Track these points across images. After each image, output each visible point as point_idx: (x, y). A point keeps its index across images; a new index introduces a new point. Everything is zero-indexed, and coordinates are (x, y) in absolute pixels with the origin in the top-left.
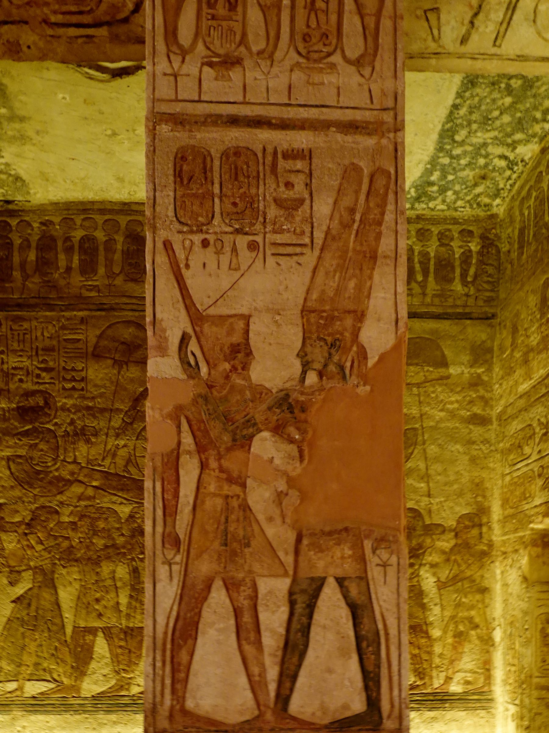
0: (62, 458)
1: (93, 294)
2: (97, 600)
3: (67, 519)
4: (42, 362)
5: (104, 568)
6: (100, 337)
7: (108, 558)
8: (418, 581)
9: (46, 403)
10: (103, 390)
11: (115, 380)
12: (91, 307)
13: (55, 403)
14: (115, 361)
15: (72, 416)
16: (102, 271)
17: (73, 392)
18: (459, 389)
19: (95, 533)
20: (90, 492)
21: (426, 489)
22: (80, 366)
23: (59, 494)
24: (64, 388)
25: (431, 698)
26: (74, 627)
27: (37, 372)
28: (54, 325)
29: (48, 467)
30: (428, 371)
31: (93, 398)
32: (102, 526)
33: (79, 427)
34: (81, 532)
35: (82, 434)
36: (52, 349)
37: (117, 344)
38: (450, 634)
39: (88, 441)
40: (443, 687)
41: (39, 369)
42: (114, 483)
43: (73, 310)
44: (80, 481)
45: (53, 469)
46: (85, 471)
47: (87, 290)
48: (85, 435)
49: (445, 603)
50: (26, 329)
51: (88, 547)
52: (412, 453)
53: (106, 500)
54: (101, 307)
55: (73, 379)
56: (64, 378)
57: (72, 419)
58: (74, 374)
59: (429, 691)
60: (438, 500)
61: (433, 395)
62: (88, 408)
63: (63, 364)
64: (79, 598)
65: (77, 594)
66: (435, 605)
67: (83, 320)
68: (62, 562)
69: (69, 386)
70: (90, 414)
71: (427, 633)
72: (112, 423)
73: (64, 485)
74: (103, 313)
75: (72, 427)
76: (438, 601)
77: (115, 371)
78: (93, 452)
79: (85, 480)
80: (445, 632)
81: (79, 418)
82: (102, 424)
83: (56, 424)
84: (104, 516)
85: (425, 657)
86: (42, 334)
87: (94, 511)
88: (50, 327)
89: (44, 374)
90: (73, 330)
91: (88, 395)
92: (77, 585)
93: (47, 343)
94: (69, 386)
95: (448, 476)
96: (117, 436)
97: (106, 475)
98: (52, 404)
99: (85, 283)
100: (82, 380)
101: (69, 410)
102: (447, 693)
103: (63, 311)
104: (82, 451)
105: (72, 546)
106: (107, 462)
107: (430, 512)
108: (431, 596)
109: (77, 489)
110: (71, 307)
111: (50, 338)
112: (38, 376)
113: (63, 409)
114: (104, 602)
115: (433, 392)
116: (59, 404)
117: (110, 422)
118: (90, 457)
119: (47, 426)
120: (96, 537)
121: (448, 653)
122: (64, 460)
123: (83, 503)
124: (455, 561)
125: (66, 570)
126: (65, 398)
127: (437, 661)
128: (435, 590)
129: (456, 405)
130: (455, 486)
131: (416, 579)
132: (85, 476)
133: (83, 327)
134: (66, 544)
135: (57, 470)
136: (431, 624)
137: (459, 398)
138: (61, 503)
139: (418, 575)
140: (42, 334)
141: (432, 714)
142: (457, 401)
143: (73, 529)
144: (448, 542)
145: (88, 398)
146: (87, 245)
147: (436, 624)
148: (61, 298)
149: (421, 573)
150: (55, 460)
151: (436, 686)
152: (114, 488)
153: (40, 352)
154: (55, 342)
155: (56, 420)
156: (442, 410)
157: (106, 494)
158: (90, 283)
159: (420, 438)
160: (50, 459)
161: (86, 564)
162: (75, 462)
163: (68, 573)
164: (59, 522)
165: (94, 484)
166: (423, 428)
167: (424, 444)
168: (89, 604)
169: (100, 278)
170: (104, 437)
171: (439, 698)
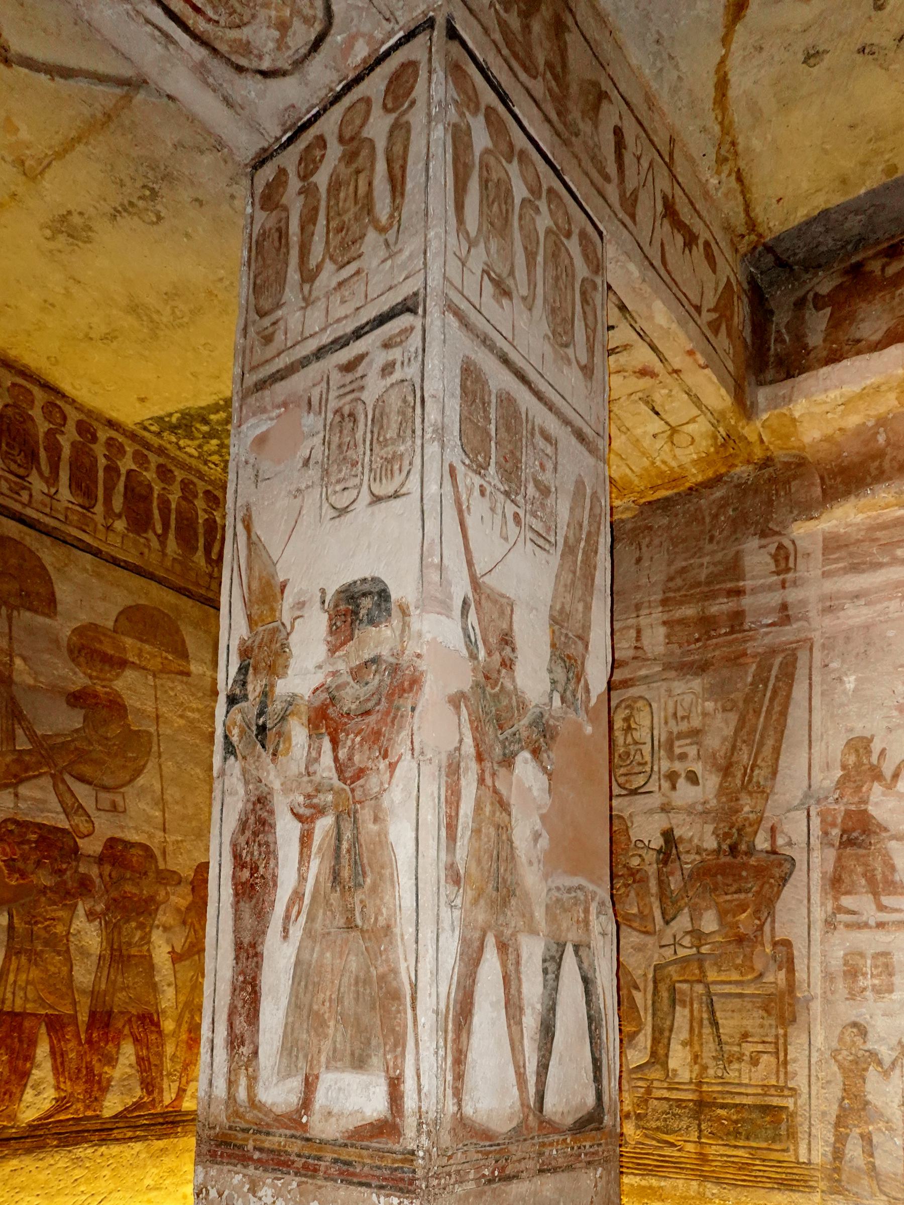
8: (148, 950)
18: (200, 694)
21: (160, 820)
25: (161, 1120)
30: (166, 658)
38: (185, 1027)
40: (175, 1103)
49: (180, 984)
52: (144, 766)
59: (159, 1110)
60: (173, 838)
61: (172, 694)
66: (169, 985)
71: (158, 1025)
76: (172, 979)
80: (179, 1025)
85: (154, 1060)
95: (185, 807)
102: (179, 1113)
107: (164, 853)
108: (164, 972)
115: (172, 689)
121: (182, 1055)
124: (192, 924)
127: (168, 1065)
128: (169, 964)
129: (197, 715)
130: (194, 824)
131: (146, 947)
136: (164, 1012)
137: (200, 706)
139: (149, 942)
141: (161, 1144)
142: (198, 710)
144: (184, 898)
147: (169, 1013)
149: (154, 938)
151: (166, 1102)
156: (181, 716)
159: (155, 748)
166: (159, 735)
167: (160, 756)
171: (171, 1119)
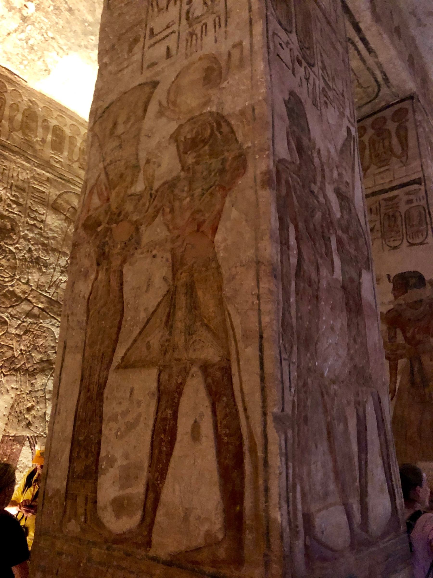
0: (18, 277)
1: (58, 165)
2: (29, 410)
3: (14, 331)
4: (14, 196)
5: (38, 380)
6: (59, 196)
7: (42, 371)
9: (13, 229)
10: (55, 235)
11: (65, 231)
12: (56, 174)
13: (19, 231)
14: (67, 218)
15: (30, 246)
16: (66, 154)
17: (34, 228)
19: (35, 348)
20: (36, 311)
22: (42, 211)
23: (10, 307)
24: (27, 223)
26: (4, 436)
27: (9, 202)
28: (27, 174)
29: (6, 282)
31: (48, 238)
32: (41, 343)
33: (35, 257)
34: (24, 345)
35: (37, 262)
36: (23, 190)
37: (69, 207)
39: (40, 270)
41: (11, 200)
42: (55, 310)
43: (44, 170)
44: (29, 301)
45: (9, 284)
46: (35, 294)
47: (55, 161)
48: (39, 264)
50: (5, 166)
51: (27, 359)
53: (47, 321)
54: (61, 176)
55: (35, 219)
56: (29, 216)
57: (30, 249)
58: (37, 215)
62: (43, 244)
63: (30, 205)
64: (12, 406)
65: (11, 402)
67: (48, 179)
68: (4, 370)
69: (32, 222)
70: (44, 250)
72: (60, 262)
73: (16, 301)
74: (63, 182)
75: (29, 255)
77: (66, 225)
78: (43, 279)
79: (34, 301)
81: (36, 250)
82: (52, 260)
83: (17, 248)
84: (44, 334)
86: (18, 175)
87: (36, 329)
88: (24, 174)
89: (14, 206)
90: (40, 183)
91: (45, 234)
92: (13, 394)
93: (20, 183)
94: (32, 222)
96: (62, 272)
97: (50, 301)
98: (17, 232)
99: (54, 156)
100: (42, 221)
101: (28, 240)
103: (35, 167)
104: (35, 277)
105: (14, 356)
106: (52, 290)
109: (26, 307)
110: (42, 167)
111: (23, 181)
112: (9, 206)
113: (25, 238)
114: (33, 412)
116: (22, 234)
117: (58, 260)
118: (40, 283)
119: (11, 248)
120: (35, 351)
122: (19, 280)
123: (29, 320)
125: (6, 378)
126: (28, 230)
132: (34, 297)
133: (48, 185)
134: (9, 354)
135: (12, 286)
138: (11, 315)
140: (18, 175)
143: (18, 341)
145: (45, 237)
146: (58, 132)
148: (35, 157)
150: (12, 278)
152: (55, 313)
153: (14, 188)
154: (26, 186)
155: (17, 245)
157: (49, 316)
158: (57, 157)
160: (8, 276)
161: (24, 375)
162: (27, 283)
163: (7, 381)
164: (7, 332)
165: (40, 306)
168: (21, 413)
169: (63, 157)
170: (52, 270)
